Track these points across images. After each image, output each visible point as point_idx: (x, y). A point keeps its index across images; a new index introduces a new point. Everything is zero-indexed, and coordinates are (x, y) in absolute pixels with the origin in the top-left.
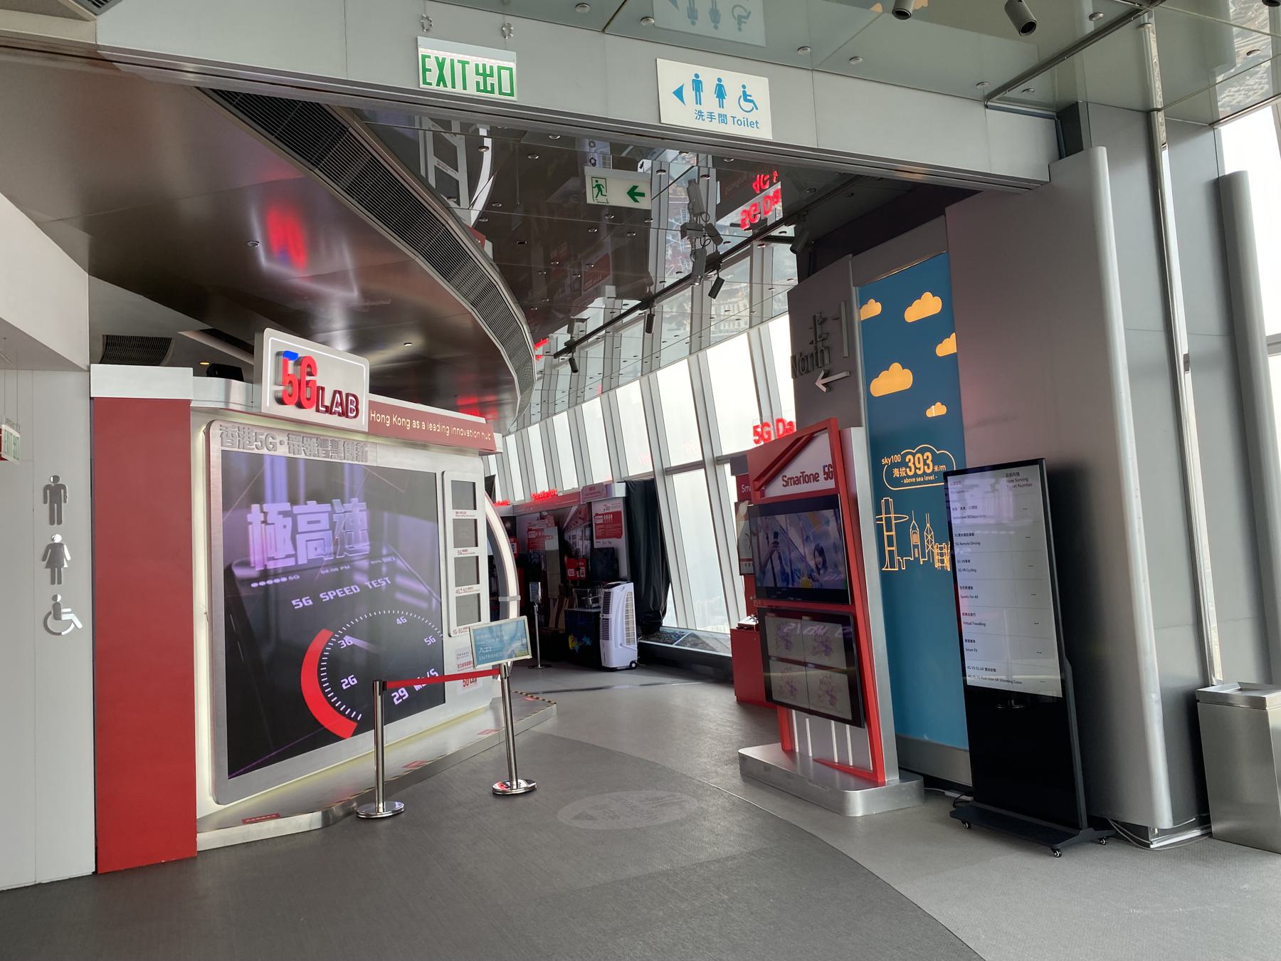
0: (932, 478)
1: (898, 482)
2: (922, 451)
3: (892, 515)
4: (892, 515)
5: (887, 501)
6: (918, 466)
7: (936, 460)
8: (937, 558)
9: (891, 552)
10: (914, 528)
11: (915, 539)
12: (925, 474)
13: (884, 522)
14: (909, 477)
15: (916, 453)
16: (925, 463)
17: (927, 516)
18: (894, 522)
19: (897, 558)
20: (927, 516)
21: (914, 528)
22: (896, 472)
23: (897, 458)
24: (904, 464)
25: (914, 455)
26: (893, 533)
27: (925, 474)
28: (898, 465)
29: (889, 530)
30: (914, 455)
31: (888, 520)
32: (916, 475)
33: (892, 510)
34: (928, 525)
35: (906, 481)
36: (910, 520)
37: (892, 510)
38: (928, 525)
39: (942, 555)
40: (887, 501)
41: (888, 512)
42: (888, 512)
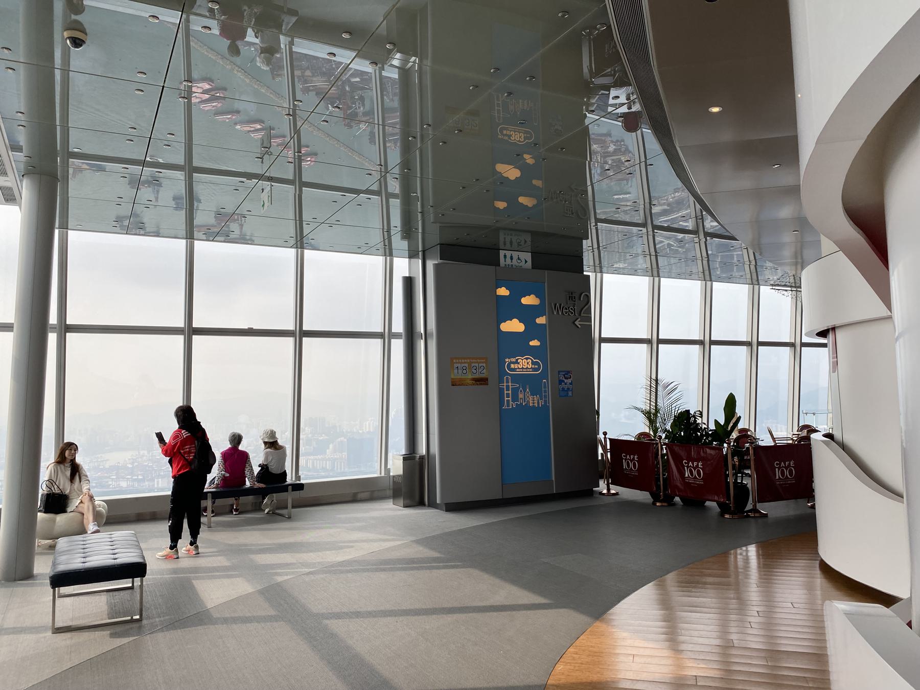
0: (531, 370)
1: (514, 370)
2: (527, 359)
3: (510, 384)
4: (510, 384)
5: (507, 378)
6: (524, 364)
7: (533, 363)
8: (531, 402)
9: (508, 401)
10: (521, 391)
11: (521, 396)
12: (527, 368)
13: (505, 387)
14: (519, 368)
15: (524, 359)
16: (528, 363)
17: (528, 386)
18: (510, 387)
19: (511, 403)
20: (528, 386)
21: (521, 391)
22: (512, 366)
23: (514, 360)
24: (517, 362)
25: (522, 360)
26: (510, 392)
27: (527, 368)
28: (513, 363)
29: (508, 390)
30: (522, 360)
31: (508, 387)
32: (523, 368)
33: (510, 381)
34: (528, 390)
35: (517, 370)
36: (520, 388)
37: (510, 381)
38: (528, 390)
39: (533, 400)
40: (507, 378)
41: (507, 382)
42: (507, 382)
